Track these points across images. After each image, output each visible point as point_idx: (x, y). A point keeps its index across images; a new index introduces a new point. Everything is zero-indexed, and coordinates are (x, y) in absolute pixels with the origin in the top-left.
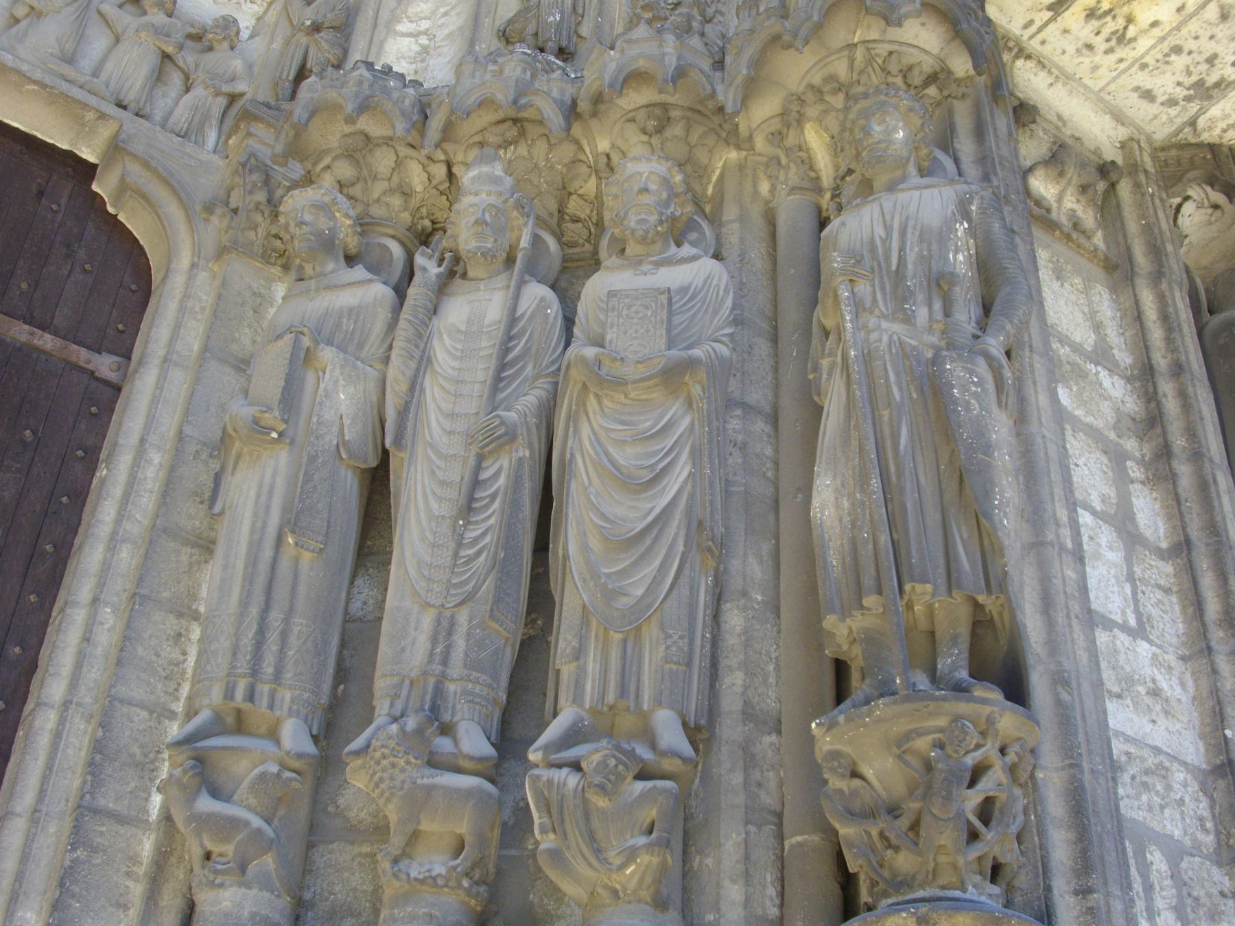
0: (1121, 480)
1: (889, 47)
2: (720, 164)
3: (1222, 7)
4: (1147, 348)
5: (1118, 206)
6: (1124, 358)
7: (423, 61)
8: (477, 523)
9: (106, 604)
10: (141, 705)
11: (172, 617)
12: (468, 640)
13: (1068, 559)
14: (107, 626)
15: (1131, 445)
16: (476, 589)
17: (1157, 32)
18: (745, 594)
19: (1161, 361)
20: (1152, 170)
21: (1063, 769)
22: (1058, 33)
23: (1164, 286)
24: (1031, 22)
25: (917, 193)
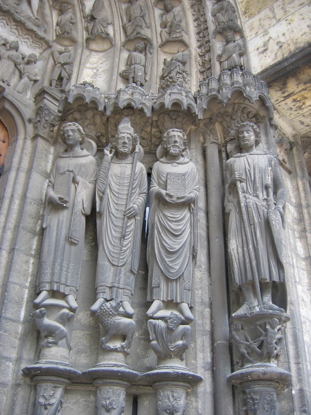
1: (245, 106)
2: (189, 129)
4: (300, 199)
5: (293, 155)
6: (294, 200)
7: (95, 78)
8: (127, 239)
9: (4, 250)
10: (17, 284)
11: (25, 256)
12: (125, 276)
14: (4, 257)
15: (296, 227)
16: (127, 260)
18: (200, 266)
19: (304, 203)
20: (301, 144)
21: (292, 328)
22: (284, 104)
23: (304, 181)
24: (278, 100)
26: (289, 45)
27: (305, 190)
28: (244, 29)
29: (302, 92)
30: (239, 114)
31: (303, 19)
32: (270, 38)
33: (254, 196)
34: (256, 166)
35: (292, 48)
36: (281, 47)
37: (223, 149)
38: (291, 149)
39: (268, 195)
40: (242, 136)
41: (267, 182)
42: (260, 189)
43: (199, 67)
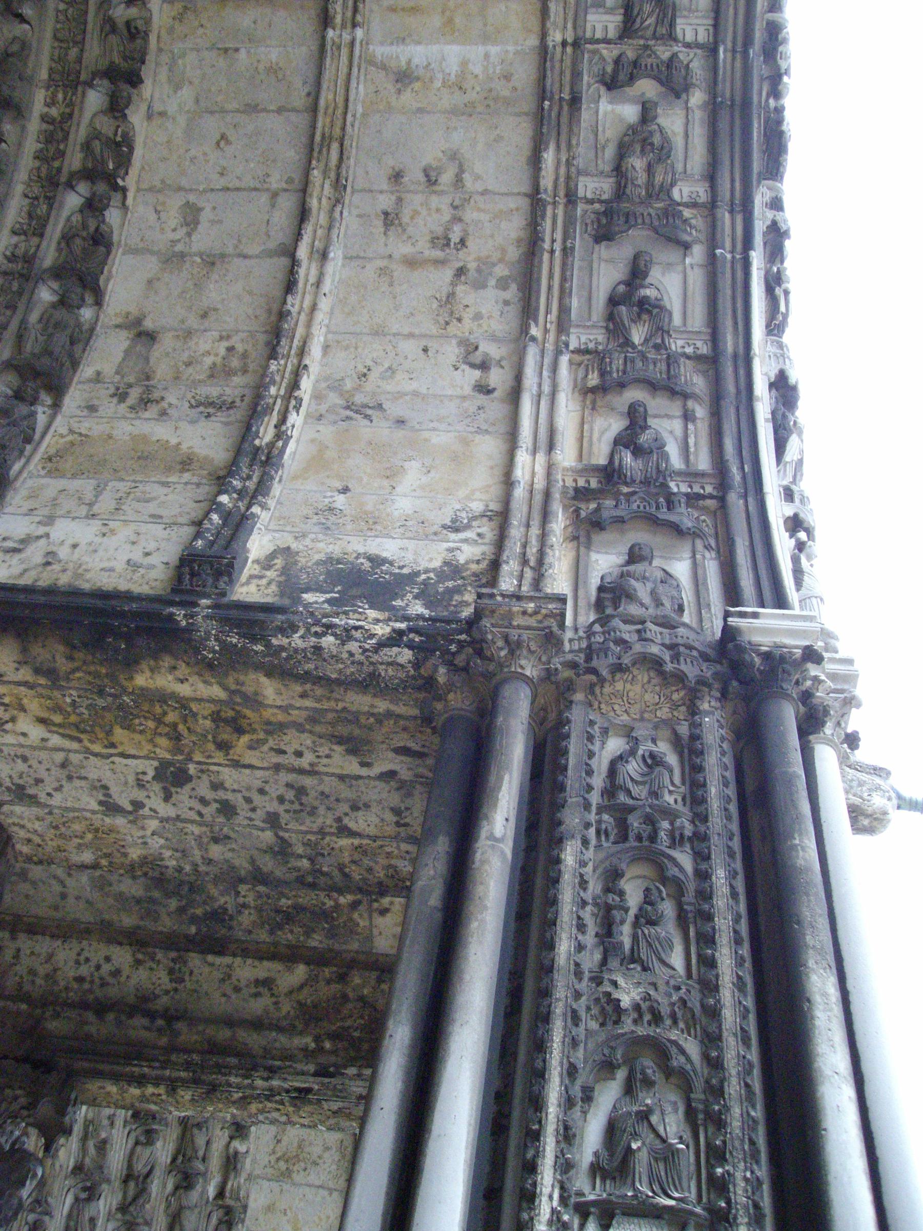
3: (66, 760)
17: (22, 740)
26: (64, 571)
28: (18, 484)
29: (22, 688)
31: (134, 543)
32: (47, 535)
35: (64, 580)
36: (48, 564)
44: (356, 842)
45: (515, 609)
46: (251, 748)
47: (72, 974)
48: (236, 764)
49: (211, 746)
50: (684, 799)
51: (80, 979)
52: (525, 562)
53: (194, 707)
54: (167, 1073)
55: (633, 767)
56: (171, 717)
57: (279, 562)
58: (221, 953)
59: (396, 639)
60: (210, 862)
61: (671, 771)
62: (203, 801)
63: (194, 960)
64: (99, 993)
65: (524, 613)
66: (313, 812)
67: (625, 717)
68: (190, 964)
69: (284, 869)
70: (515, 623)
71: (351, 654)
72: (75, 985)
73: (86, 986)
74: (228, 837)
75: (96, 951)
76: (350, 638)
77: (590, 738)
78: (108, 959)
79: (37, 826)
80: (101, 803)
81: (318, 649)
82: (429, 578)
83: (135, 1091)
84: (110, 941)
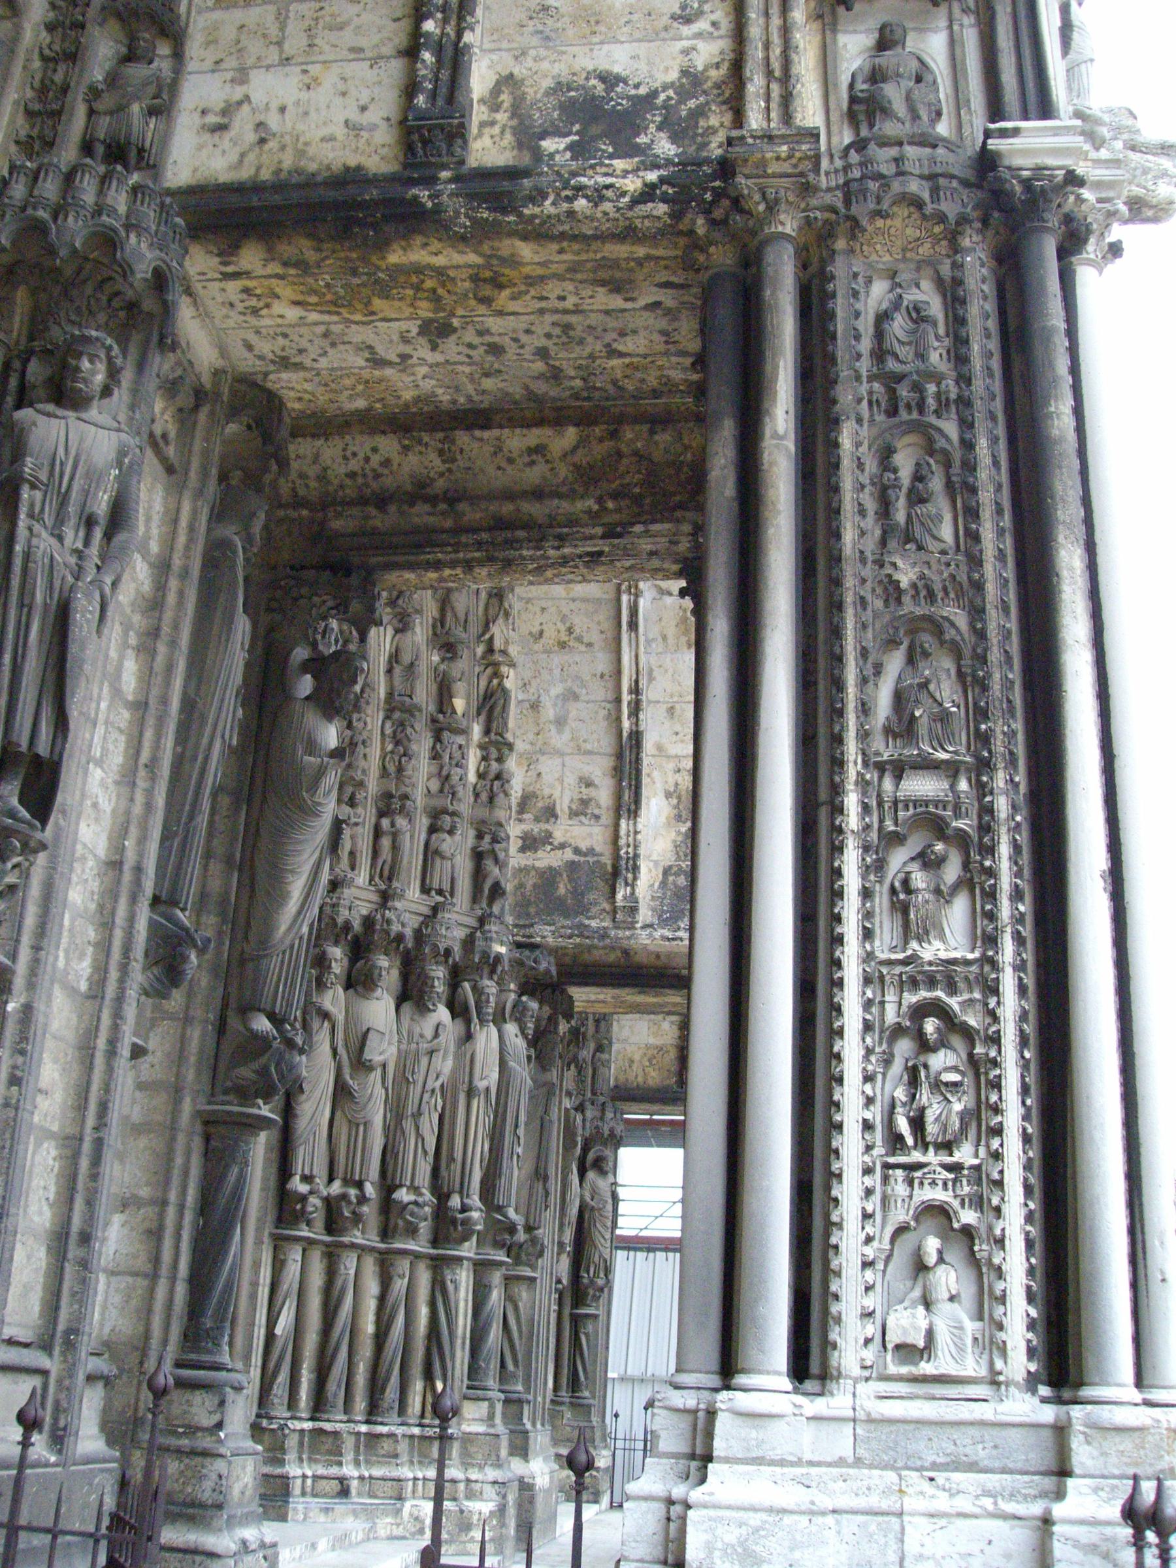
0: (125, 645)
5: (195, 422)
6: (154, 547)
13: (89, 725)
15: (137, 618)
17: (279, 321)
19: (177, 562)
24: (204, 274)
25: (93, 428)
26: (283, 148)
27: (191, 529)
28: (190, 30)
30: (89, 289)
31: (344, 94)
32: (247, 98)
33: (52, 534)
34: (83, 458)
35: (288, 161)
36: (262, 141)
37: (17, 364)
38: (196, 408)
39: (87, 543)
40: (74, 362)
41: (95, 509)
42: (73, 522)
43: (30, 94)
44: (627, 360)
45: (769, 155)
46: (513, 298)
47: (342, 470)
48: (500, 313)
49: (473, 303)
50: (948, 352)
51: (352, 475)
52: (769, 73)
53: (452, 273)
54: (461, 555)
55: (899, 325)
56: (429, 284)
57: (505, 98)
58: (486, 427)
59: (648, 194)
60: (484, 392)
61: (935, 324)
62: (470, 346)
63: (463, 438)
64: (374, 485)
65: (778, 158)
66: (581, 342)
67: (887, 258)
68: (459, 442)
69: (558, 390)
70: (770, 171)
71: (605, 214)
72: (348, 482)
73: (360, 480)
74: (500, 371)
75: (361, 444)
76: (602, 198)
77: (855, 294)
78: (375, 450)
79: (306, 386)
80: (367, 360)
81: (571, 214)
82: (669, 98)
83: (432, 575)
84: (373, 432)
